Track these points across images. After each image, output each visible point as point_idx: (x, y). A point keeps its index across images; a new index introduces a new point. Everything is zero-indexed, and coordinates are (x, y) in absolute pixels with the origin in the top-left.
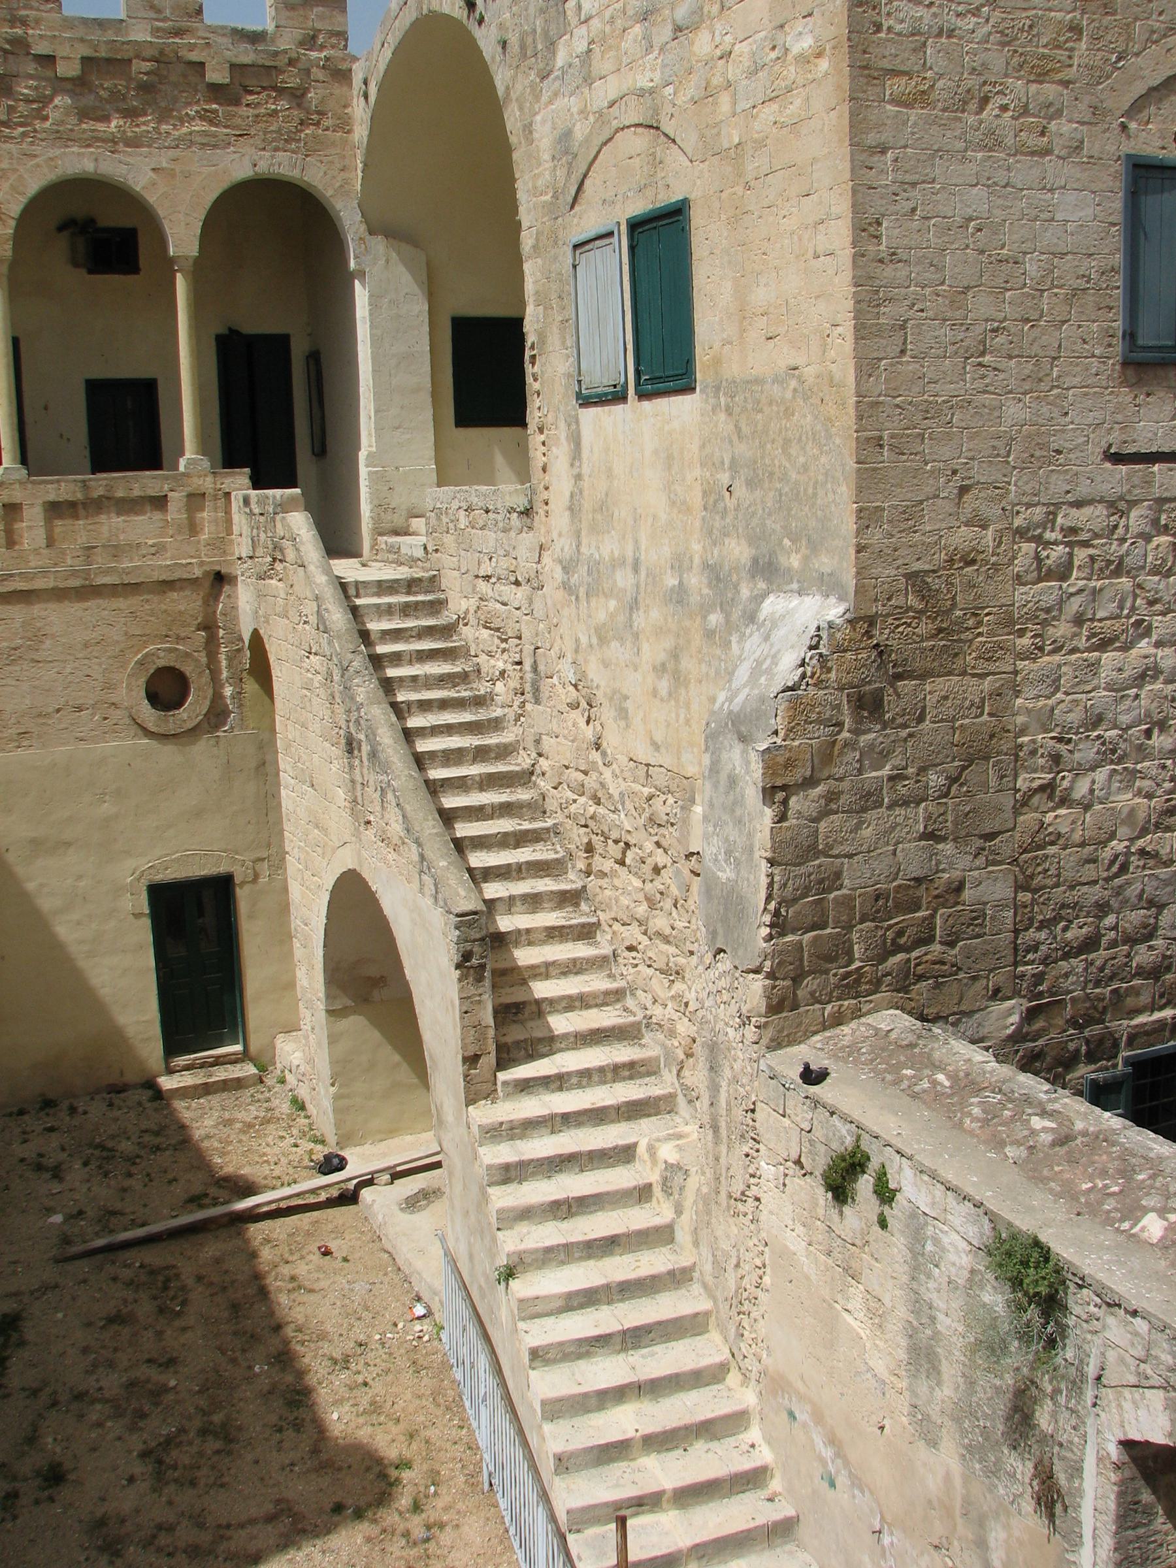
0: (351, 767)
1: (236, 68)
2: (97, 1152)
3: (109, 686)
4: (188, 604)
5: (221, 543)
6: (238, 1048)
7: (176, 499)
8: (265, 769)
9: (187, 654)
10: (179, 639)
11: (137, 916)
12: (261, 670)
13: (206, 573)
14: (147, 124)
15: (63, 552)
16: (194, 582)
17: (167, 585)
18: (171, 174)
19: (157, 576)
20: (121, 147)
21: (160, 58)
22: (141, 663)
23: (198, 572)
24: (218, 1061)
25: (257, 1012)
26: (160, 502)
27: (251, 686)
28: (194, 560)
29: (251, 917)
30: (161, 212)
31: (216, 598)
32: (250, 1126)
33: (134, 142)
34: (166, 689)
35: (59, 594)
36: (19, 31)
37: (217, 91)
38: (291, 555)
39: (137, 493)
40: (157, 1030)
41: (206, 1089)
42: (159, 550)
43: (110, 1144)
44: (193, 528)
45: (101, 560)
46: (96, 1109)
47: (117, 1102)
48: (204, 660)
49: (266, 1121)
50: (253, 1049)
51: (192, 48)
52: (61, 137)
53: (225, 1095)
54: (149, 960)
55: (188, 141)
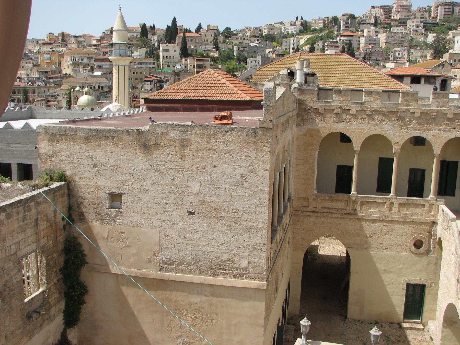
0: (457, 285)
1: (455, 114)
2: (386, 338)
3: (406, 242)
4: (426, 228)
5: (436, 215)
6: (419, 321)
7: (427, 205)
8: (437, 264)
9: (424, 237)
10: (423, 234)
11: (403, 289)
12: (440, 243)
13: (431, 221)
14: (433, 126)
15: (401, 213)
16: (428, 223)
17: (422, 223)
18: (436, 137)
19: (420, 221)
20: (426, 131)
21: (438, 112)
22: (413, 238)
23: (429, 221)
24: (415, 322)
25: (426, 314)
26: (423, 205)
27: (437, 246)
28: (429, 218)
29: (428, 294)
30: (433, 145)
31: (433, 227)
32: (420, 341)
33: (429, 130)
34: (418, 244)
35: (399, 222)
36: (408, 107)
37: (449, 119)
38: (451, 232)
39: (418, 203)
40: (403, 313)
41: (411, 329)
42: (422, 215)
43: (389, 337)
44: (430, 211)
45: (408, 216)
46: (387, 326)
47: (391, 327)
48: (427, 239)
49: (424, 341)
50: (423, 321)
51: (445, 110)
52: (413, 129)
53: (415, 331)
54: (404, 299)
55: (442, 130)
